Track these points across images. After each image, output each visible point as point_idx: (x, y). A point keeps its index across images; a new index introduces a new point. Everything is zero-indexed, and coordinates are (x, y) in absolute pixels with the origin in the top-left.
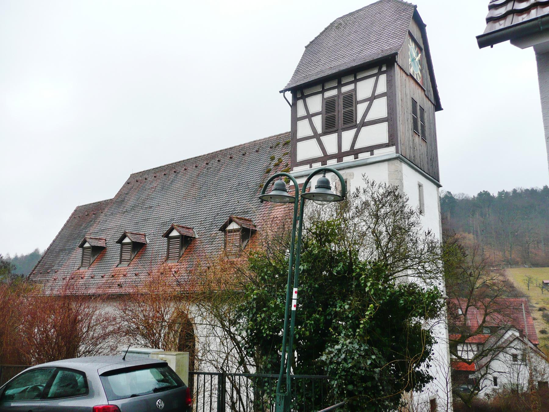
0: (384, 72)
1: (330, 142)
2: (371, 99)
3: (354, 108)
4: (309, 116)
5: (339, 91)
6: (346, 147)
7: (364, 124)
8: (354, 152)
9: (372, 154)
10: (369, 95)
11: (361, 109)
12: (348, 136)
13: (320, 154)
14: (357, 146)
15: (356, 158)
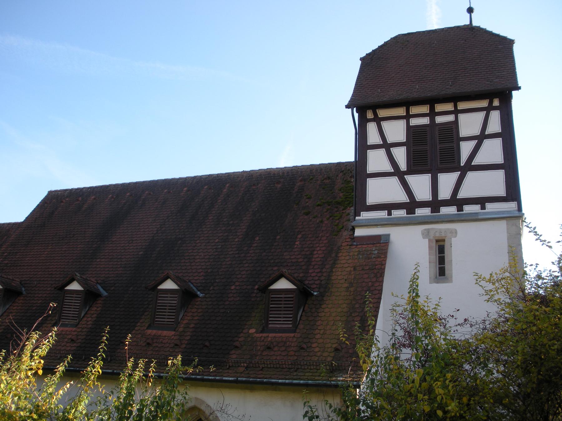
0: (495, 108)
1: (421, 185)
2: (481, 138)
3: (455, 145)
4: (387, 146)
5: (432, 120)
6: (445, 193)
7: (470, 167)
8: (456, 201)
9: (483, 208)
10: (477, 131)
11: (466, 148)
12: (447, 181)
13: (403, 198)
14: (462, 194)
15: (390, 214)
